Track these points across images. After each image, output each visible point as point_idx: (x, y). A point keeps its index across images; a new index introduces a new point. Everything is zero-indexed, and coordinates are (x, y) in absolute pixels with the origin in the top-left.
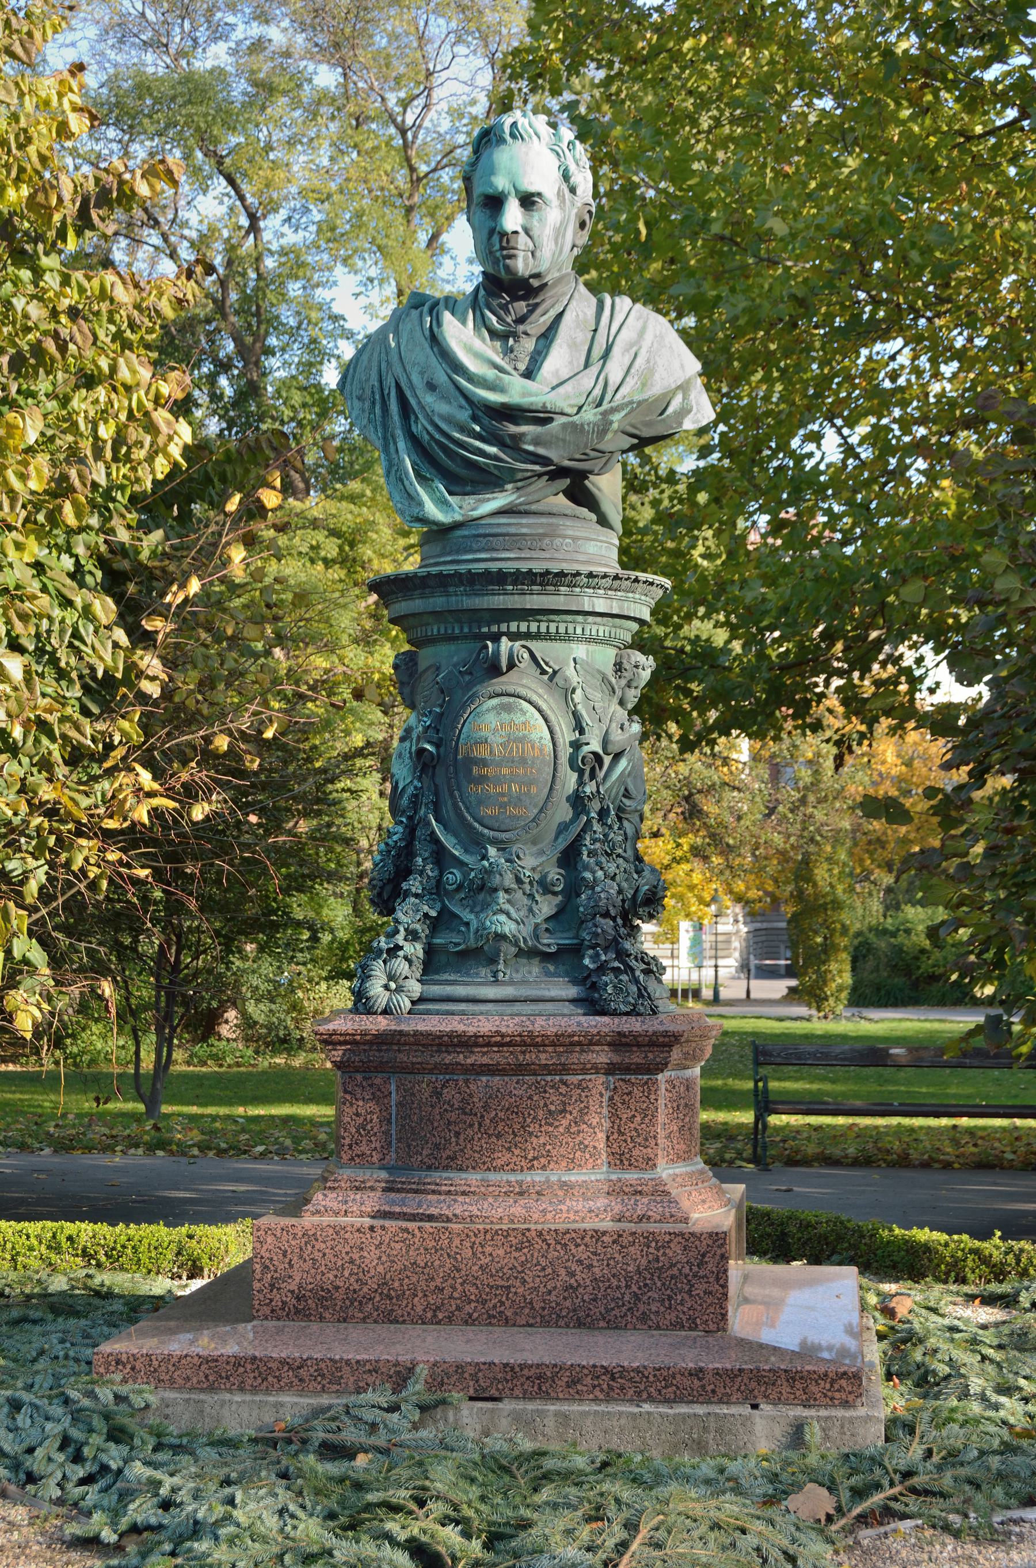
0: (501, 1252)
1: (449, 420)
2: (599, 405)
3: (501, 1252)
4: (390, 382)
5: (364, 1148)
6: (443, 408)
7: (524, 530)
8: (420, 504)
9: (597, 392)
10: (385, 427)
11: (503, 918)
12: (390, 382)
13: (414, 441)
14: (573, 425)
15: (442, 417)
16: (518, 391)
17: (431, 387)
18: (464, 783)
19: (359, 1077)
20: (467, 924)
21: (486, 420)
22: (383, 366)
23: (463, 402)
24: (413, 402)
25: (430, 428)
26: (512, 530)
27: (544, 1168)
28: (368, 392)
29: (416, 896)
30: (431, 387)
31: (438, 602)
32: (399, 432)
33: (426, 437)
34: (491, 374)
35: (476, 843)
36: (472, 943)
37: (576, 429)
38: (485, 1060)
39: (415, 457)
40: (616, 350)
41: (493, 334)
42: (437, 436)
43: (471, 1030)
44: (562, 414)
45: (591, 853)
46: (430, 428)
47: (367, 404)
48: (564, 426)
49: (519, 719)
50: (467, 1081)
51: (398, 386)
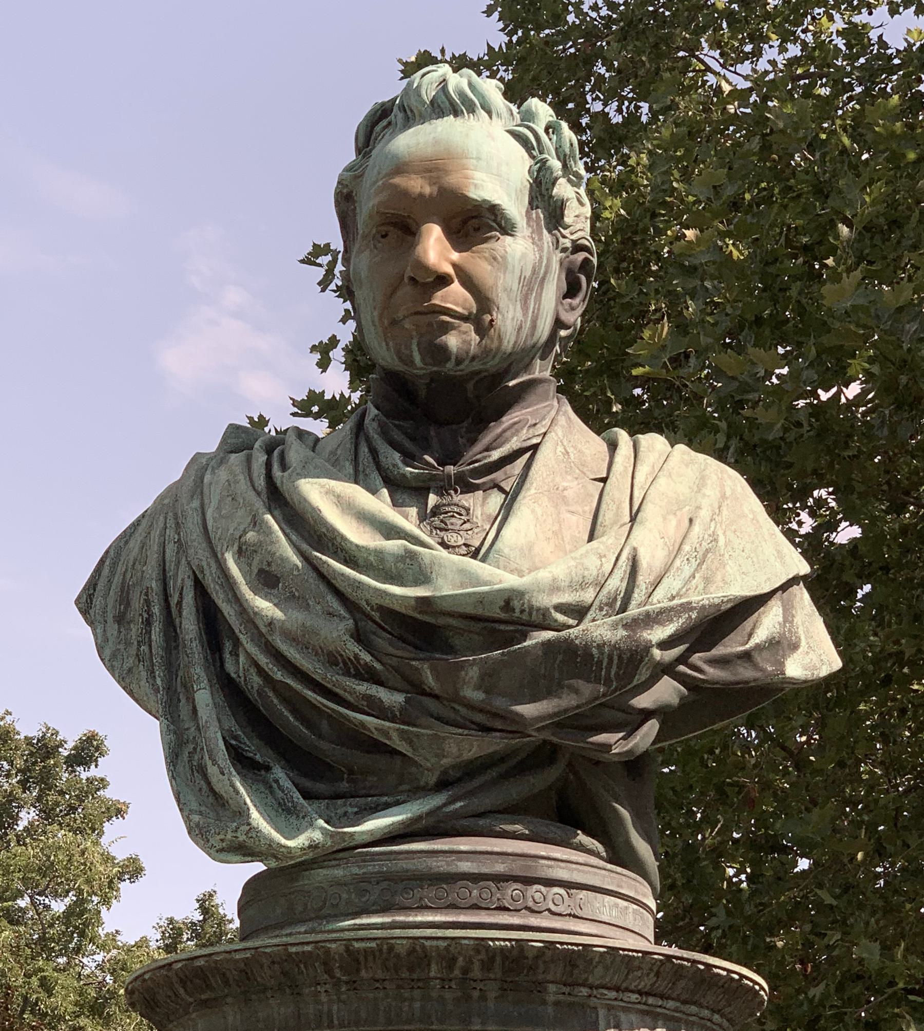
2: (623, 609)
4: (182, 578)
7: (465, 866)
8: (242, 814)
9: (617, 583)
10: (171, 667)
12: (182, 578)
13: (231, 691)
14: (568, 642)
16: (453, 575)
21: (382, 641)
22: (171, 549)
23: (335, 604)
24: (227, 609)
25: (263, 660)
26: (441, 865)
28: (137, 603)
33: (256, 680)
34: (395, 545)
37: (573, 659)
39: (230, 723)
40: (650, 512)
42: (278, 675)
46: (263, 660)
47: (135, 630)
48: (547, 644)
51: (200, 587)
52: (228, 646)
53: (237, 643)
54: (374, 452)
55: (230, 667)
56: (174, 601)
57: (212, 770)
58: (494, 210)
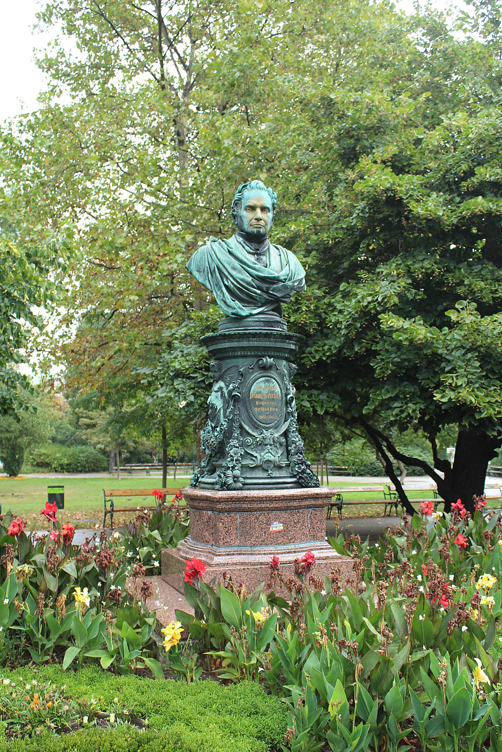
0: (288, 574)
1: (243, 280)
3: (288, 574)
5: (228, 539)
6: (241, 276)
11: (270, 455)
12: (213, 265)
13: (227, 287)
15: (240, 279)
17: (234, 269)
18: (253, 407)
19: (226, 514)
20: (256, 457)
22: (210, 261)
25: (235, 283)
27: (293, 542)
29: (236, 447)
30: (234, 269)
31: (244, 344)
32: (222, 283)
33: (232, 286)
35: (256, 427)
36: (259, 463)
37: (286, 287)
38: (277, 505)
41: (249, 253)
43: (274, 495)
44: (281, 281)
45: (293, 432)
46: (235, 283)
49: (272, 385)
50: (268, 513)
52: (225, 279)
53: (227, 278)
54: (244, 247)
55: (226, 283)
56: (212, 269)
57: (227, 301)
58: (268, 208)
